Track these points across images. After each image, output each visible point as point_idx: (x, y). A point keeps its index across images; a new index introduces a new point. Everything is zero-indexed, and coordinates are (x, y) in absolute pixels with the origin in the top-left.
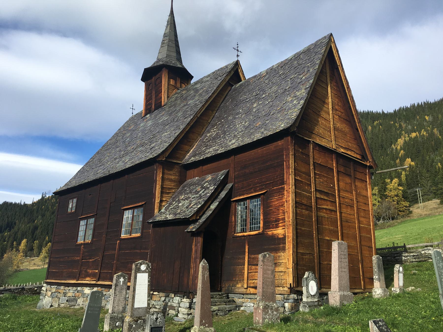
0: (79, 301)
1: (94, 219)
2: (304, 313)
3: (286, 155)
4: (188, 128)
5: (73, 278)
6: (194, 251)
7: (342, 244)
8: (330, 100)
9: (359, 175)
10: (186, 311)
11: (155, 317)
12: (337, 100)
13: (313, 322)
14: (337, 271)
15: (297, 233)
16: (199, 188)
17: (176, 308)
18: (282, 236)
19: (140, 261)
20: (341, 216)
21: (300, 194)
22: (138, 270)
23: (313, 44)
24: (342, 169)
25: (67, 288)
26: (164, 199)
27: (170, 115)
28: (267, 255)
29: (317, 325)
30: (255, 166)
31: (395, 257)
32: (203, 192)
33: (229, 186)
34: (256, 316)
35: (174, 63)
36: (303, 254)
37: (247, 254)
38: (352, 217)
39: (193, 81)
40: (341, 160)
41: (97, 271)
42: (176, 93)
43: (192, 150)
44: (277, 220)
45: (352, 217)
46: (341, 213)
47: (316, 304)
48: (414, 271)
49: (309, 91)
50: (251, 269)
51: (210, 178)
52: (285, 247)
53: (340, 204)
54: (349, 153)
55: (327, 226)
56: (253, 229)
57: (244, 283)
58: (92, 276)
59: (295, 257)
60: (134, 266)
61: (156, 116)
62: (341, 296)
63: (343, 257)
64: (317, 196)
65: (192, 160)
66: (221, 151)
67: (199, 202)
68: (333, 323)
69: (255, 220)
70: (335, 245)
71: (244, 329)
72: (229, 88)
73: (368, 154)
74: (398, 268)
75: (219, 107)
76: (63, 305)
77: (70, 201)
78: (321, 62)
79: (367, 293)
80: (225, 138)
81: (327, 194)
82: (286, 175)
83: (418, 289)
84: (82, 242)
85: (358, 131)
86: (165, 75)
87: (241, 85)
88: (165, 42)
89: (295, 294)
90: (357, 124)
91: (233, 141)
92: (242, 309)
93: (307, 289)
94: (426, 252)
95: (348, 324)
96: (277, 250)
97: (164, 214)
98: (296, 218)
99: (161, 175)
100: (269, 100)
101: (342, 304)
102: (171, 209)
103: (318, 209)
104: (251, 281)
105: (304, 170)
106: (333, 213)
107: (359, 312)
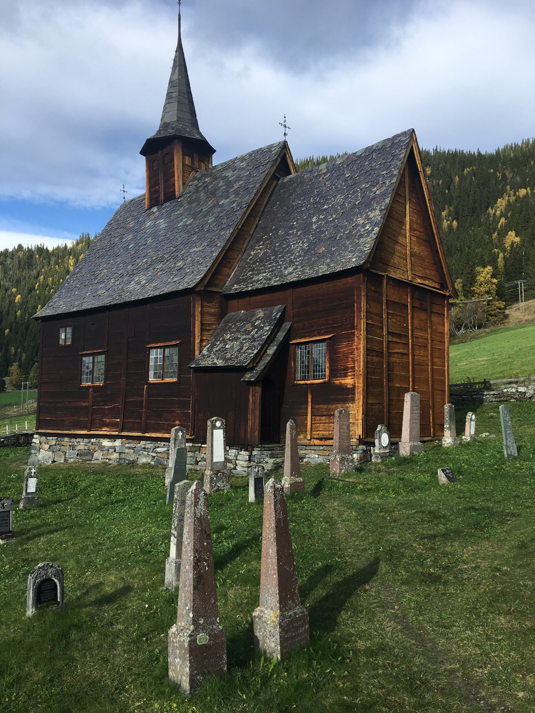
0: (96, 455)
1: (103, 356)
2: (376, 464)
3: (357, 296)
4: (228, 246)
5: (83, 429)
6: (251, 401)
7: (415, 396)
8: (408, 219)
9: (436, 309)
10: (246, 464)
11: (257, 470)
12: (416, 216)
13: (385, 471)
14: (409, 422)
15: (367, 382)
16: (249, 327)
17: (233, 461)
18: (352, 387)
19: (215, 418)
20: (413, 359)
21: (371, 339)
22: (214, 427)
23: (389, 139)
24: (417, 304)
25: (73, 440)
26: (205, 338)
27: (195, 216)
28: (343, 411)
29: (390, 474)
30: (318, 304)
31: (472, 396)
32: (256, 333)
33: (287, 325)
34: (333, 468)
36: (372, 404)
37: (310, 404)
38: (425, 359)
39: (217, 160)
40: (417, 292)
41: (119, 420)
42: (195, 179)
43: (233, 274)
44: (346, 369)
45: (425, 359)
46: (413, 356)
47: (388, 454)
48: (492, 414)
49: (385, 214)
50: (315, 420)
51: (261, 314)
52: (354, 398)
53: (413, 345)
54: (426, 282)
55: (398, 372)
56: (316, 377)
57: (307, 434)
58: (113, 425)
59: (365, 408)
60: (209, 423)
61: (169, 214)
62: (411, 446)
63: (415, 408)
64: (389, 340)
65: (236, 289)
66: (275, 282)
67: (254, 346)
68: (405, 471)
69: (319, 367)
70: (408, 397)
71: (323, 479)
72: (275, 183)
73: (448, 281)
74: (470, 416)
75: (263, 211)
76: (72, 460)
77: (61, 330)
78: (399, 172)
79: (437, 441)
80: (277, 262)
81: (399, 336)
82: (357, 319)
83: (493, 436)
84: (89, 384)
85: (438, 253)
86: (176, 148)
87: (291, 180)
88: (174, 95)
89: (363, 445)
90: (438, 245)
91: (291, 269)
92: (305, 460)
93: (380, 441)
94: (509, 390)
95: (419, 472)
96: (345, 401)
97: (208, 357)
98: (367, 367)
99: (200, 309)
100: (334, 216)
101: (412, 454)
102: (217, 351)
103: (390, 354)
104: (315, 432)
105: (375, 311)
106: (405, 357)
107: (428, 461)
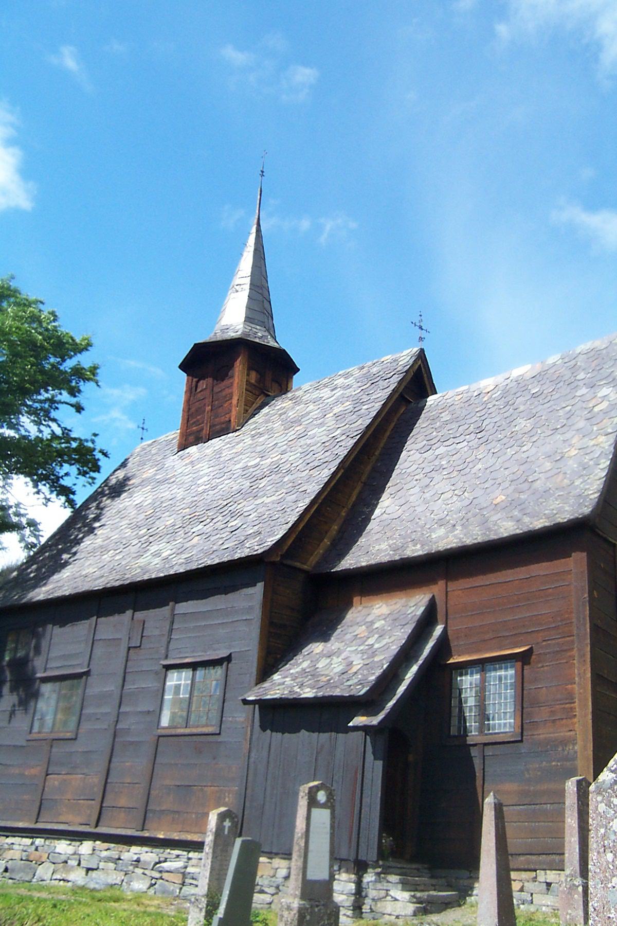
0: (40, 871)
35: (259, 335)
